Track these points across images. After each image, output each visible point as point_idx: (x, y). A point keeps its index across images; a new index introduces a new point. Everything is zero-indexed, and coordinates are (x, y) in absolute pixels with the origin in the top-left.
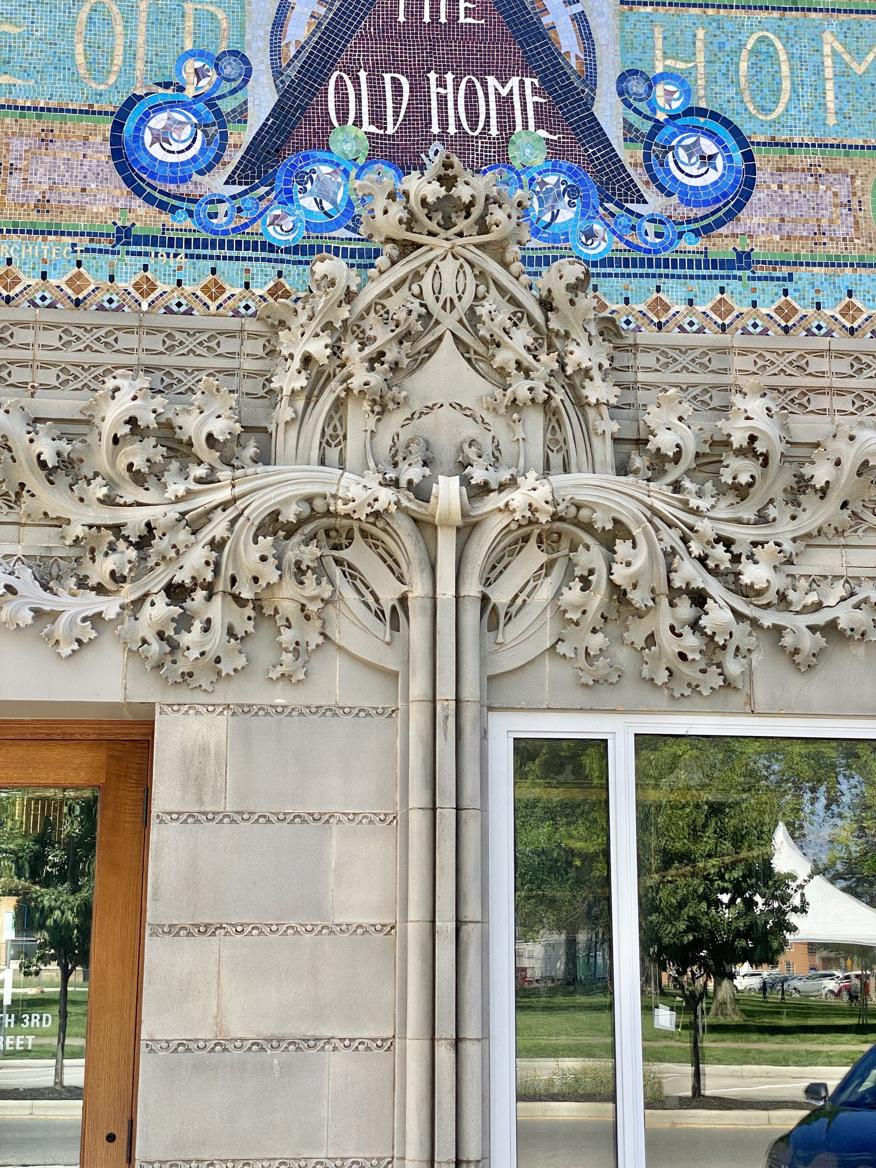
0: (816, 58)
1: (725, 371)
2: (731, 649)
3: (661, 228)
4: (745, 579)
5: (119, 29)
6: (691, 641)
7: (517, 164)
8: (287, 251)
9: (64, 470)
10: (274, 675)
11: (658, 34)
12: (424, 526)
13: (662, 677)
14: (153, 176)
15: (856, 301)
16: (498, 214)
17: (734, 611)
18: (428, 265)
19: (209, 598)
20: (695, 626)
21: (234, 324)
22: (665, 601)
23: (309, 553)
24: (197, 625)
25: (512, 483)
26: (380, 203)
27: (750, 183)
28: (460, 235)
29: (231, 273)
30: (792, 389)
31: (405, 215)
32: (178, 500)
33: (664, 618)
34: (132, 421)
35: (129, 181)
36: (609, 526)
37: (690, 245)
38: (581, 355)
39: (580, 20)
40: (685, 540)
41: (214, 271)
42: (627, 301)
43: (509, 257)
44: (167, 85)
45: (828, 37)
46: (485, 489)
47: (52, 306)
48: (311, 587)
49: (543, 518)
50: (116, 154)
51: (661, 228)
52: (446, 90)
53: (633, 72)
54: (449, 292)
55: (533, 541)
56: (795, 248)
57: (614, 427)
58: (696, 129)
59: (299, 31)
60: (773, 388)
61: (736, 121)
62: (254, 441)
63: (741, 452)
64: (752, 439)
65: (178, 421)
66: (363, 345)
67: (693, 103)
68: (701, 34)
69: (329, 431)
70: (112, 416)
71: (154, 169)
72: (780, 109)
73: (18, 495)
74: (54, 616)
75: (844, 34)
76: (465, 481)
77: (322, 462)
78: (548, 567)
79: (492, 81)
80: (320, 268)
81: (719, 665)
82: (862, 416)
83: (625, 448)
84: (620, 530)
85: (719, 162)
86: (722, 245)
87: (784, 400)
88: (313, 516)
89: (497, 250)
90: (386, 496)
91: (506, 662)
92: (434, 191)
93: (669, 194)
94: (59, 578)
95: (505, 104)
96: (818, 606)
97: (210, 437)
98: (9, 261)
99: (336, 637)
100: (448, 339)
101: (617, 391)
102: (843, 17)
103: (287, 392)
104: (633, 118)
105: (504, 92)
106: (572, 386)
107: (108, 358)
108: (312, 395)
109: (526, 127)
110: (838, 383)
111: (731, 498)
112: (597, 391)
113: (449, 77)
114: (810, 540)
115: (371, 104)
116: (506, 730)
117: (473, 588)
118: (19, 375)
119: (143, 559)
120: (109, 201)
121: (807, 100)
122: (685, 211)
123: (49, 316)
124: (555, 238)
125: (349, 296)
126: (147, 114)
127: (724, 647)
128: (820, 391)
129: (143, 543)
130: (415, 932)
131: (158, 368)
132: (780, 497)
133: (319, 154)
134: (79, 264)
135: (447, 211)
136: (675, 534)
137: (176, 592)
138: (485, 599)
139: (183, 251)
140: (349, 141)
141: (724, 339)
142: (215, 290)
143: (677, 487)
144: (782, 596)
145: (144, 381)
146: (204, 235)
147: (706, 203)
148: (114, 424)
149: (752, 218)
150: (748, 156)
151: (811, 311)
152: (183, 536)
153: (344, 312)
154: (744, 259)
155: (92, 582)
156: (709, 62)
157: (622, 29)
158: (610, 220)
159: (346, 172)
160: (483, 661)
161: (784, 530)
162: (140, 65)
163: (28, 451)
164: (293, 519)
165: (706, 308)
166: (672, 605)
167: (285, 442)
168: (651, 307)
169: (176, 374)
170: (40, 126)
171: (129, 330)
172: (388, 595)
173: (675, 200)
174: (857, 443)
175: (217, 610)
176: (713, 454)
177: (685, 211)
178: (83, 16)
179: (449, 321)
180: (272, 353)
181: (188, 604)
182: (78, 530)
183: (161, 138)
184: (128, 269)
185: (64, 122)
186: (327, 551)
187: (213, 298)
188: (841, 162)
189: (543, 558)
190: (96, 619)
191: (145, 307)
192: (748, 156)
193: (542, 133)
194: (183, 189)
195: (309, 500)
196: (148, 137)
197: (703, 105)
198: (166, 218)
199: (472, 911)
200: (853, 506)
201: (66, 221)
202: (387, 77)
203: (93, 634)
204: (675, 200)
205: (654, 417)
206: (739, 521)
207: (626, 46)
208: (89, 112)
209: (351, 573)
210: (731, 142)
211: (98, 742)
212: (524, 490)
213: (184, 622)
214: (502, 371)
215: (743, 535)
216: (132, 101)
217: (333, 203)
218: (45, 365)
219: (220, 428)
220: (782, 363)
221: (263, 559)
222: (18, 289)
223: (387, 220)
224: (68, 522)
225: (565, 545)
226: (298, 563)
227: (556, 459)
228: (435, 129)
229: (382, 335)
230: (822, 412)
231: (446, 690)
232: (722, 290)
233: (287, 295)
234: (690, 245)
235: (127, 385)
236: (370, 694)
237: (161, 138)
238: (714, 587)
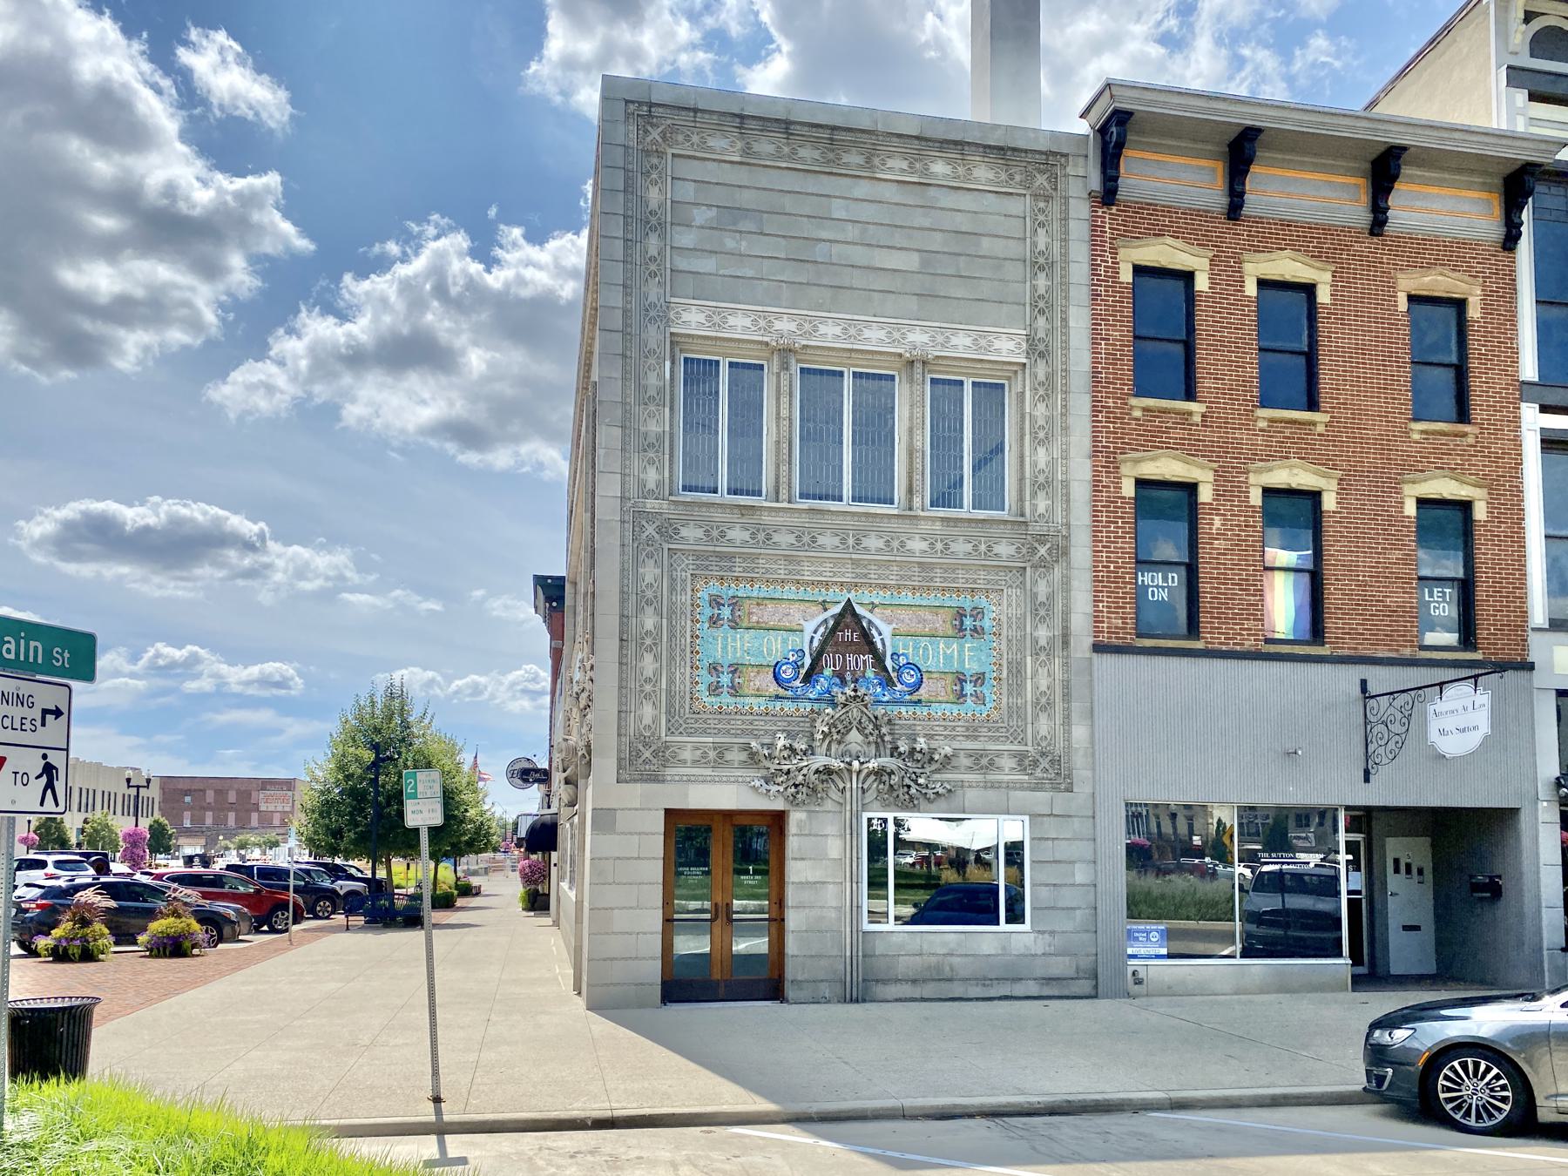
9: (770, 757)
38: (884, 730)
52: (850, 658)
59: (816, 644)
62: (810, 751)
112: (887, 738)
114: (933, 772)
120: (773, 688)
137: (796, 786)
140: (828, 672)
149: (922, 691)
161: (928, 770)
167: (818, 750)
172: (841, 785)
175: (804, 790)
184: (778, 705)
205: (899, 743)
219: (804, 747)
236: (837, 808)
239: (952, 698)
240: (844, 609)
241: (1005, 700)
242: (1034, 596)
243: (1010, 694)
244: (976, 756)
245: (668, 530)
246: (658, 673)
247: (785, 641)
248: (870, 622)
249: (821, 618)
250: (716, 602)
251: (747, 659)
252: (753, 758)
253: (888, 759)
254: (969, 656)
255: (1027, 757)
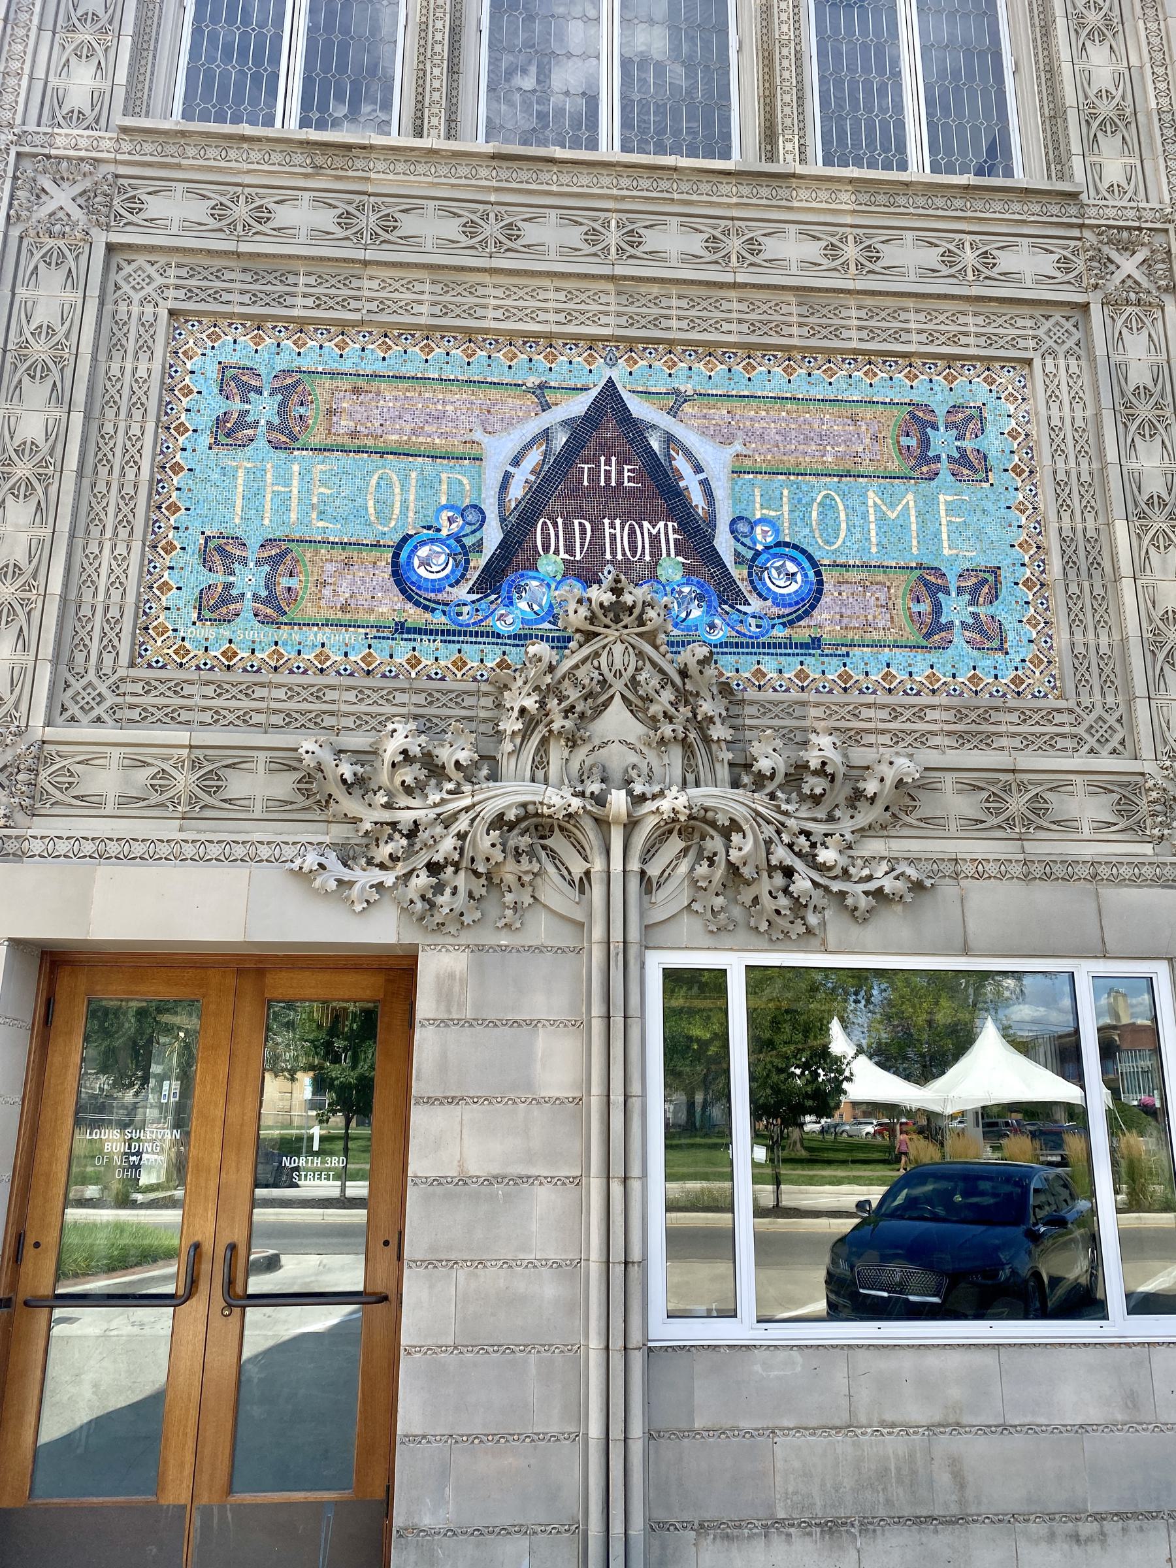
0: (863, 508)
1: (804, 718)
2: (811, 907)
3: (760, 622)
4: (820, 859)
5: (397, 491)
6: (783, 902)
7: (663, 579)
8: (509, 637)
9: (359, 785)
10: (500, 925)
11: (757, 492)
12: (602, 824)
13: (764, 926)
14: (419, 588)
15: (893, 671)
16: (651, 613)
17: (813, 881)
18: (604, 647)
19: (456, 872)
20: (786, 891)
21: (473, 686)
22: (765, 874)
23: (524, 841)
24: (448, 891)
25: (661, 794)
26: (572, 606)
27: (820, 592)
28: (626, 627)
29: (471, 652)
30: (850, 729)
31: (589, 614)
32: (435, 805)
33: (765, 885)
34: (405, 752)
35: (403, 591)
36: (727, 823)
37: (779, 633)
39: (705, 483)
40: (778, 832)
41: (460, 651)
42: (737, 671)
43: (659, 642)
44: (429, 528)
45: (871, 494)
46: (643, 798)
47: (351, 675)
48: (525, 865)
49: (682, 818)
50: (395, 573)
51: (760, 622)
52: (615, 531)
53: (741, 518)
54: (618, 665)
55: (675, 833)
56: (850, 635)
57: (730, 756)
58: (782, 556)
59: (517, 491)
60: (837, 729)
61: (810, 550)
62: (487, 766)
63: (816, 773)
64: (824, 764)
65: (436, 752)
66: (560, 701)
67: (781, 539)
68: (786, 492)
69: (537, 759)
70: (391, 749)
71: (420, 583)
72: (840, 542)
73: (327, 802)
74: (351, 884)
75: (882, 493)
76: (630, 793)
77: (533, 780)
78: (685, 851)
79: (646, 524)
80: (532, 650)
81: (803, 918)
82: (898, 748)
83: (737, 770)
84: (734, 826)
85: (799, 577)
86: (801, 633)
87: (844, 737)
88: (527, 816)
89: (650, 637)
90: (576, 803)
91: (658, 915)
92: (608, 598)
93: (765, 599)
94: (354, 858)
95: (654, 539)
96: (870, 878)
97: (457, 763)
98: (323, 645)
99: (542, 898)
100: (618, 697)
101: (732, 731)
102: (881, 481)
103: (509, 732)
104: (740, 548)
105: (654, 532)
106: (701, 728)
107: (389, 709)
108: (526, 734)
109: (669, 555)
110: (881, 726)
111: (809, 804)
112: (718, 732)
113: (618, 522)
115: (565, 540)
116: (657, 962)
117: (635, 866)
118: (329, 721)
119: (411, 845)
120: (390, 605)
121: (858, 536)
122: (775, 610)
123: (350, 681)
124: (688, 629)
125: (551, 668)
126: (416, 547)
127: (806, 906)
128: (868, 731)
129: (412, 834)
130: (596, 1103)
131: (422, 716)
132: (843, 803)
133: (531, 573)
134: (370, 647)
135: (617, 611)
136: (772, 828)
137: (434, 868)
138: (643, 873)
139: (439, 638)
140: (550, 564)
141: (804, 696)
142: (460, 664)
143: (772, 796)
144: (845, 871)
145: (412, 725)
146: (453, 627)
147: (790, 605)
148: (393, 755)
149: (821, 615)
150: (818, 574)
151: (861, 677)
152: (439, 830)
153: (548, 679)
154: (816, 643)
155: (377, 861)
156: (791, 511)
157: (733, 489)
158: (726, 616)
159: (549, 585)
160: (642, 915)
161: (846, 826)
162: (411, 514)
163: (334, 773)
164: (513, 818)
165: (791, 675)
166: (770, 877)
167: (508, 766)
168: (754, 675)
169: (435, 720)
170: (344, 555)
171: (402, 691)
173: (769, 603)
174: (895, 766)
176: (797, 773)
177: (775, 610)
178: (374, 482)
179: (618, 685)
180: (499, 706)
181: (442, 876)
182: (368, 826)
183: (425, 563)
184: (403, 650)
185: (360, 552)
186: (536, 841)
187: (459, 669)
188: (881, 578)
189: (682, 845)
190: (379, 886)
191: (413, 675)
192: (818, 574)
193: (680, 559)
194: (440, 597)
195: (524, 805)
196: (416, 562)
197: (787, 539)
198: (428, 615)
199: (635, 1089)
200: (894, 809)
201: (362, 617)
202: (576, 522)
203: (377, 897)
204: (769, 603)
205: (756, 749)
206: (815, 820)
207: (736, 501)
208: (377, 545)
209: (553, 855)
210: (806, 564)
211: (379, 970)
212: (669, 799)
213: (439, 889)
214: (654, 719)
215: (817, 828)
216: (406, 539)
217: (540, 606)
218: (346, 714)
219: (464, 756)
220: (843, 712)
221: (493, 845)
222: (328, 663)
223: (577, 617)
224: (361, 820)
225: (697, 836)
226: (517, 848)
227: (690, 777)
228: (608, 556)
229: (573, 694)
230: (871, 745)
231: (617, 935)
232: (802, 663)
233: (508, 667)
234: (779, 633)
235: (402, 729)
236: (566, 937)
237: (425, 563)
238: (799, 865)
239: (911, 634)
240: (596, 405)
241: (1062, 638)
242: (1119, 372)
243: (1075, 621)
244: (993, 789)
245: (108, 198)
246: (40, 551)
247: (428, 485)
248: (670, 439)
249: (534, 426)
250: (237, 381)
251: (318, 527)
252: (312, 793)
253: (727, 791)
254: (951, 526)
255: (1137, 789)
